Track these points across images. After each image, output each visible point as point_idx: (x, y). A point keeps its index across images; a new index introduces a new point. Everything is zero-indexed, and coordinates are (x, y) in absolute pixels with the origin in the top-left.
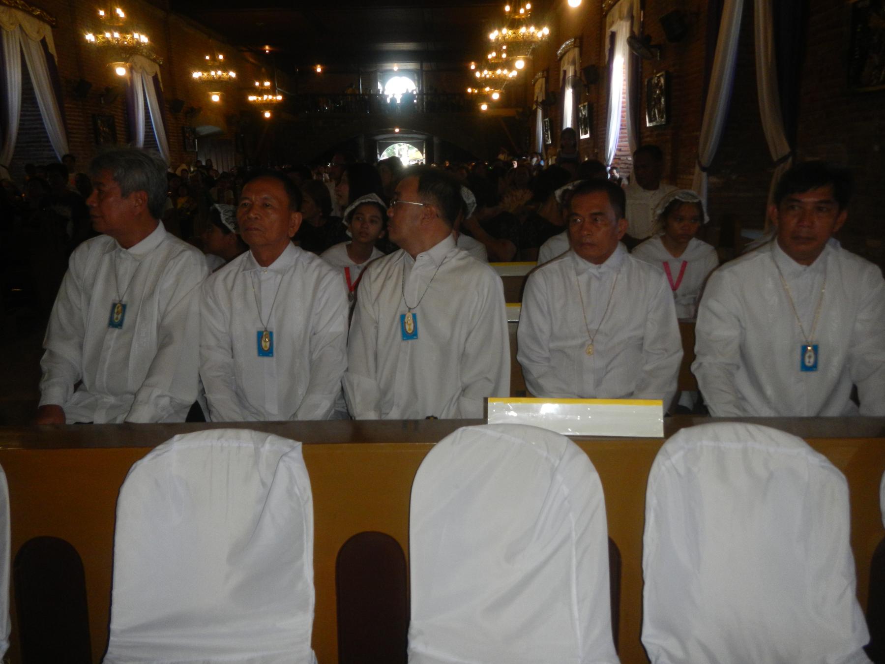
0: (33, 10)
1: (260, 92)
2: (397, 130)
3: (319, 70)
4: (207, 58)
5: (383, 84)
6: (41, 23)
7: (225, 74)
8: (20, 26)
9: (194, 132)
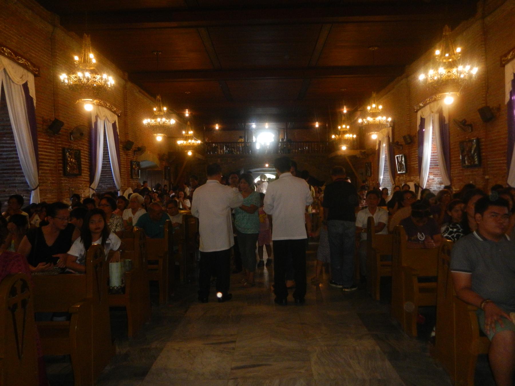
0: (18, 59)
1: (186, 138)
2: (267, 165)
3: (217, 127)
4: (155, 109)
5: (256, 137)
6: (26, 71)
7: (168, 121)
8: (4, 69)
9: (138, 164)
